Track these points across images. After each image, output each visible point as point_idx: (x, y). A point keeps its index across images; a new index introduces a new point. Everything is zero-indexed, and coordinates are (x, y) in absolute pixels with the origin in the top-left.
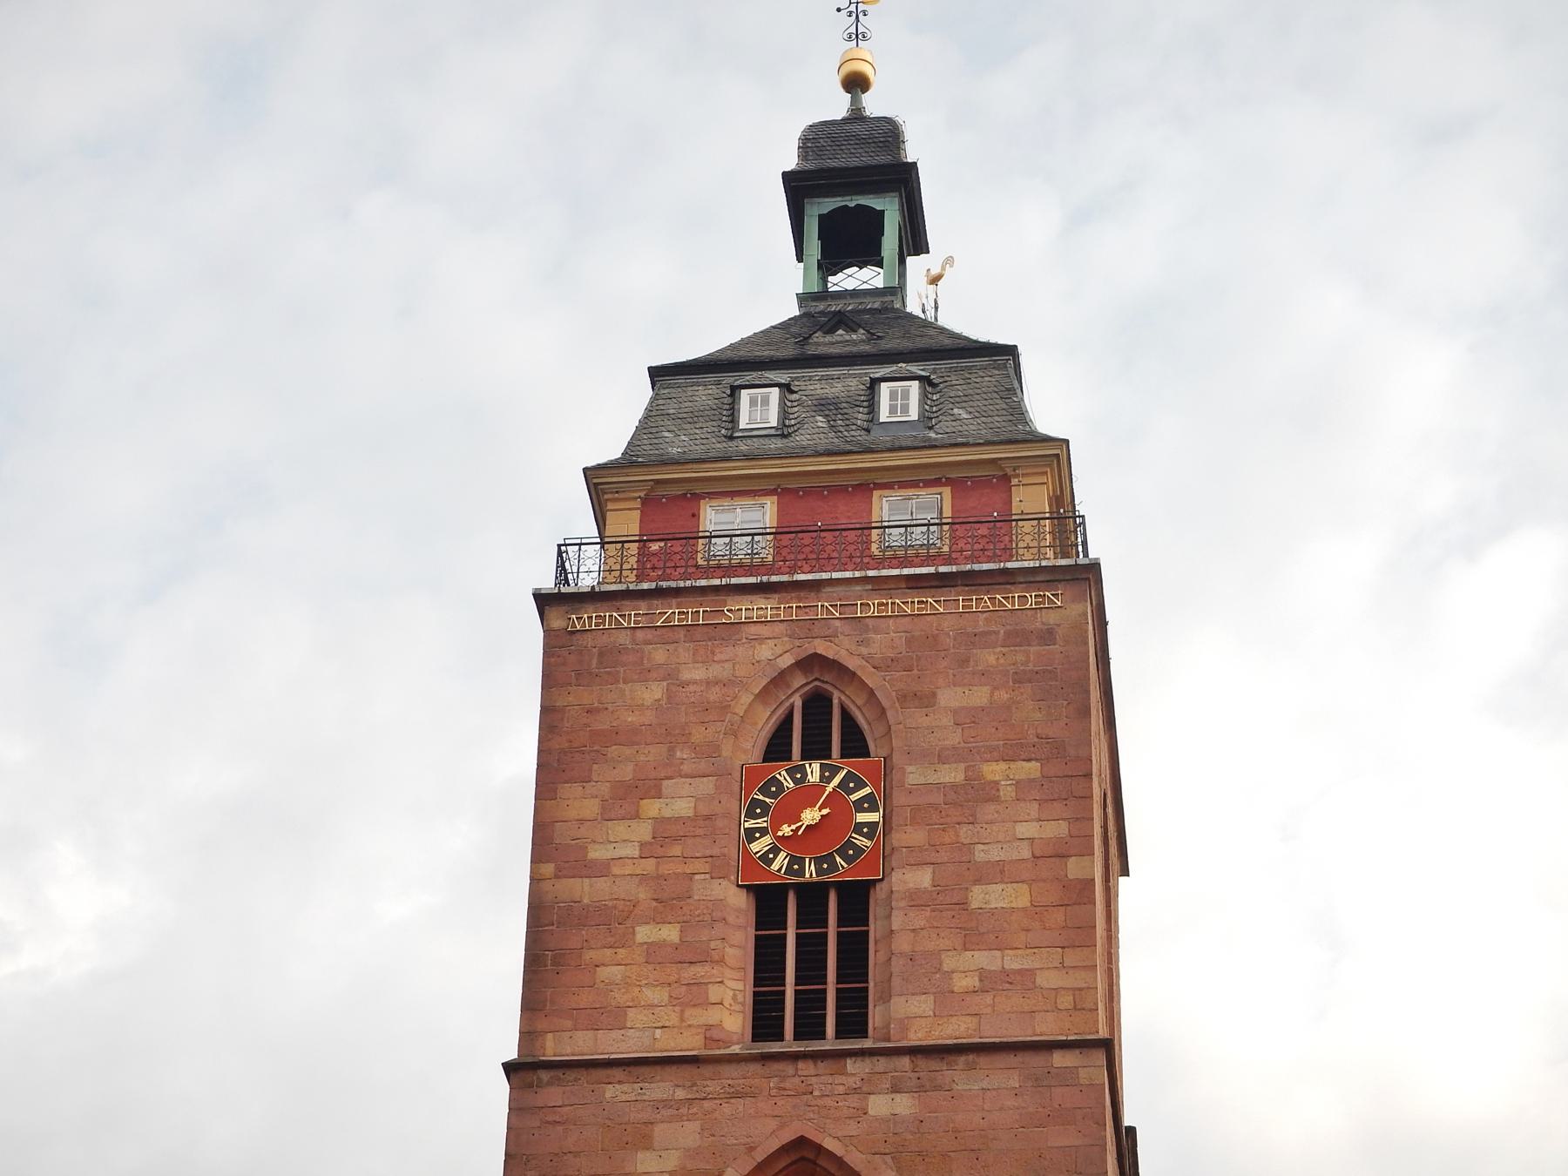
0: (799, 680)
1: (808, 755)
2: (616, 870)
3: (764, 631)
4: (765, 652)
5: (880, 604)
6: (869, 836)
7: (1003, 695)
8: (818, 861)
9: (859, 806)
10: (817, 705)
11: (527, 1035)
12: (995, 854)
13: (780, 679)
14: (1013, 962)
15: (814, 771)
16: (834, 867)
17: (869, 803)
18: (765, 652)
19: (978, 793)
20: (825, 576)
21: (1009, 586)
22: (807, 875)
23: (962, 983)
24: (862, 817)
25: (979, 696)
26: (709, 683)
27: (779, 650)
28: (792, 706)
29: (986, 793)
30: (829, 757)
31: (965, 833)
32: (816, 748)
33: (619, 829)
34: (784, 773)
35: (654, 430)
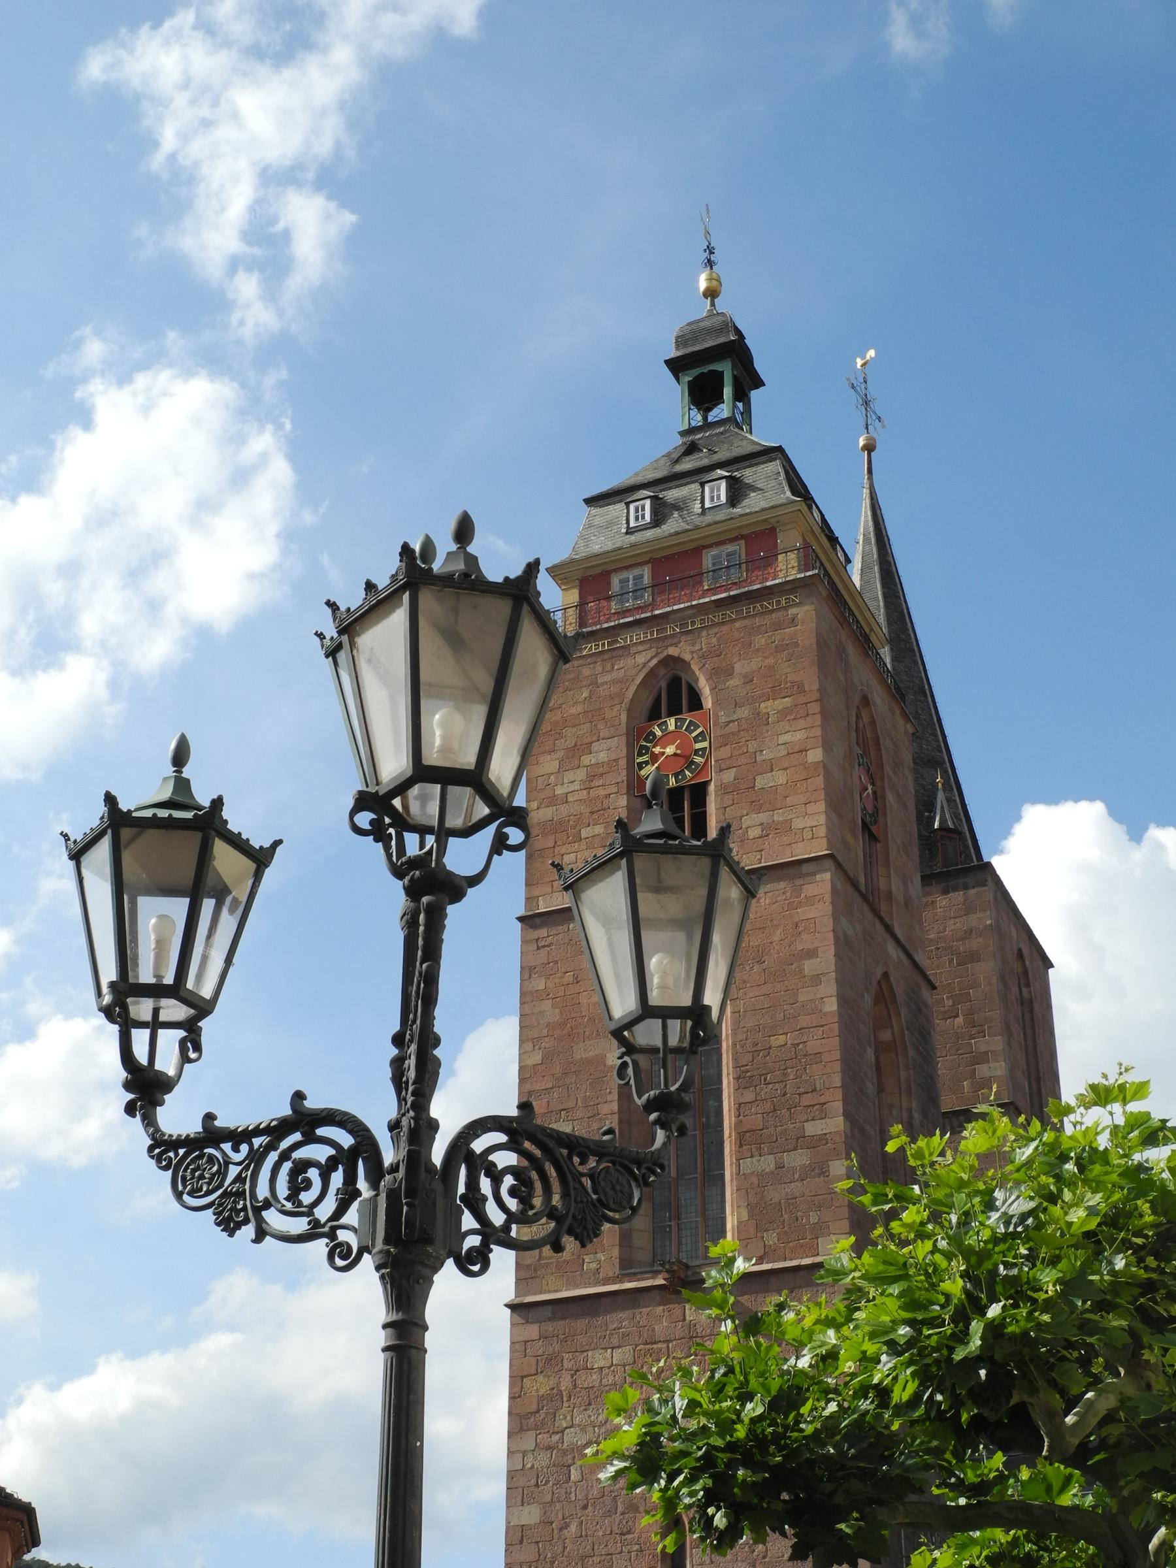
0: (662, 671)
1: (670, 715)
2: (570, 799)
3: (641, 648)
4: (641, 659)
5: (701, 620)
6: (702, 756)
7: (771, 661)
8: (676, 775)
9: (696, 740)
10: (675, 684)
11: (530, 900)
12: (767, 754)
13: (652, 673)
14: (778, 817)
15: (671, 723)
16: (685, 776)
17: (701, 737)
18: (641, 659)
19: (761, 720)
20: (669, 609)
21: (770, 596)
22: (671, 784)
23: (754, 833)
24: (698, 746)
25: (754, 663)
26: (614, 682)
27: (648, 657)
28: (661, 687)
29: (761, 720)
30: (681, 713)
31: (752, 746)
32: (674, 710)
33: (570, 776)
34: (656, 727)
35: (587, 537)
